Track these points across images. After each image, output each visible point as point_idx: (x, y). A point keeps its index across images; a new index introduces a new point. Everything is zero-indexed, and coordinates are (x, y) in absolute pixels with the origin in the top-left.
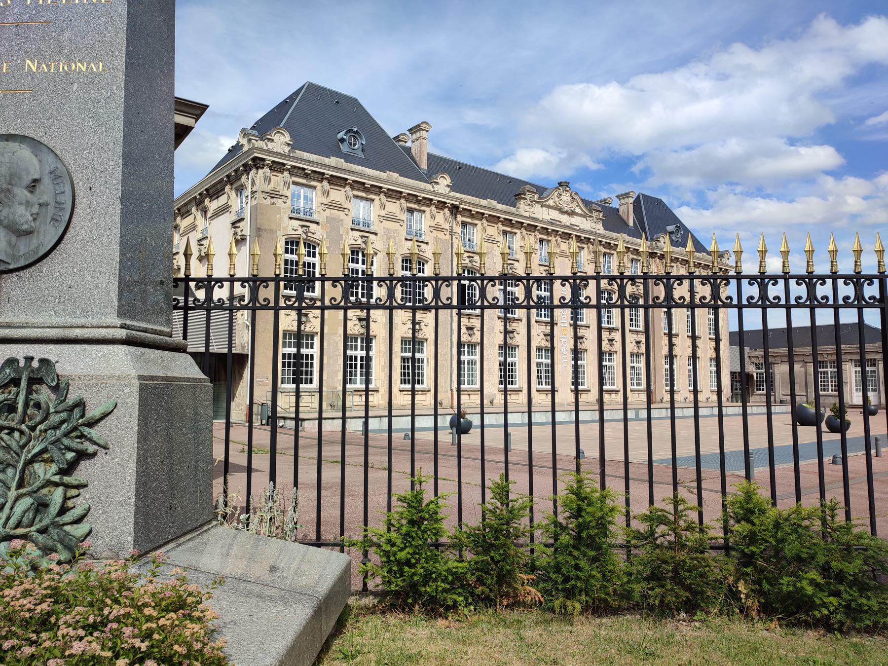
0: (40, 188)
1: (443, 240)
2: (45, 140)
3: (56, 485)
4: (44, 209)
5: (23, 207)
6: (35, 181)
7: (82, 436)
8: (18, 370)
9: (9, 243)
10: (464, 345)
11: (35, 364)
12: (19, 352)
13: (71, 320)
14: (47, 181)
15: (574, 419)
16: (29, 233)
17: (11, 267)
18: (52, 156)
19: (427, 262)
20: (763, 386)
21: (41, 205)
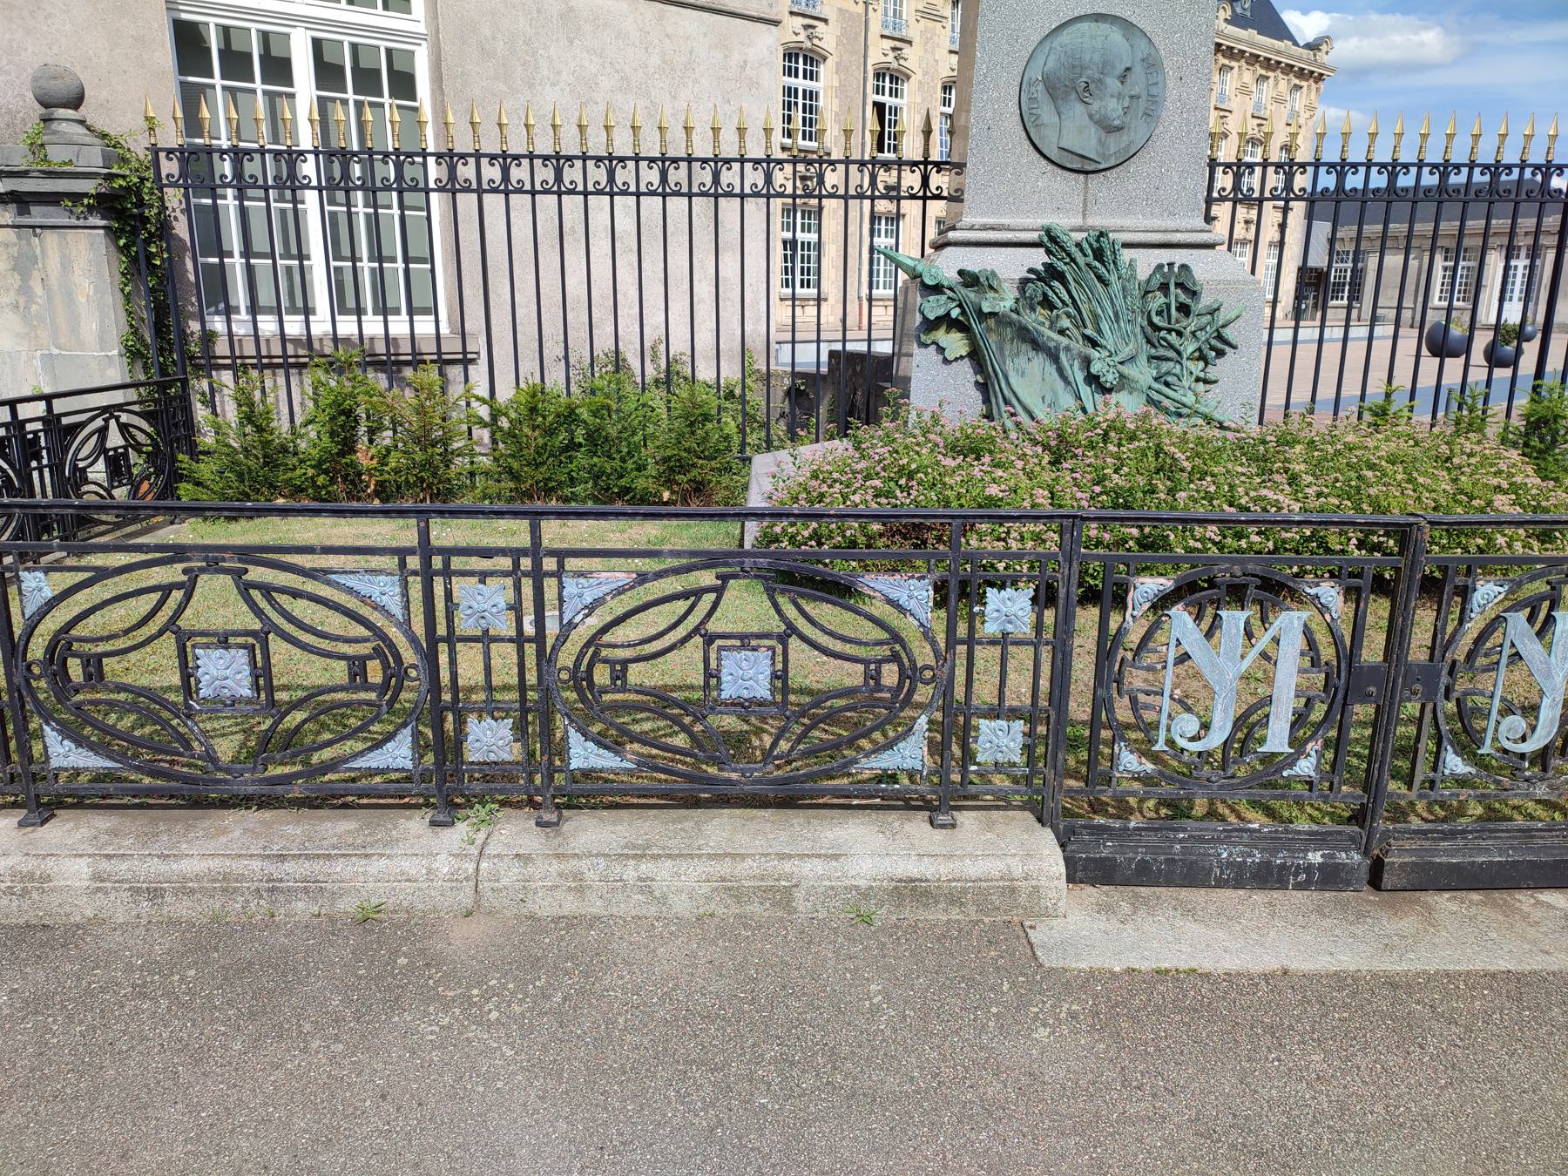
0: (1129, 79)
1: (851, 15)
2: (1133, 20)
3: (1198, 380)
4: (1135, 101)
5: (1115, 100)
6: (1128, 69)
7: (1220, 337)
8: (1163, 275)
9: (1099, 140)
10: (880, 218)
11: (1176, 270)
12: (1164, 256)
13: (1171, 224)
14: (1138, 69)
15: (1317, 337)
16: (1119, 129)
17: (1102, 167)
18: (1145, 41)
19: (825, 59)
20: (1343, 292)
21: (1132, 97)
